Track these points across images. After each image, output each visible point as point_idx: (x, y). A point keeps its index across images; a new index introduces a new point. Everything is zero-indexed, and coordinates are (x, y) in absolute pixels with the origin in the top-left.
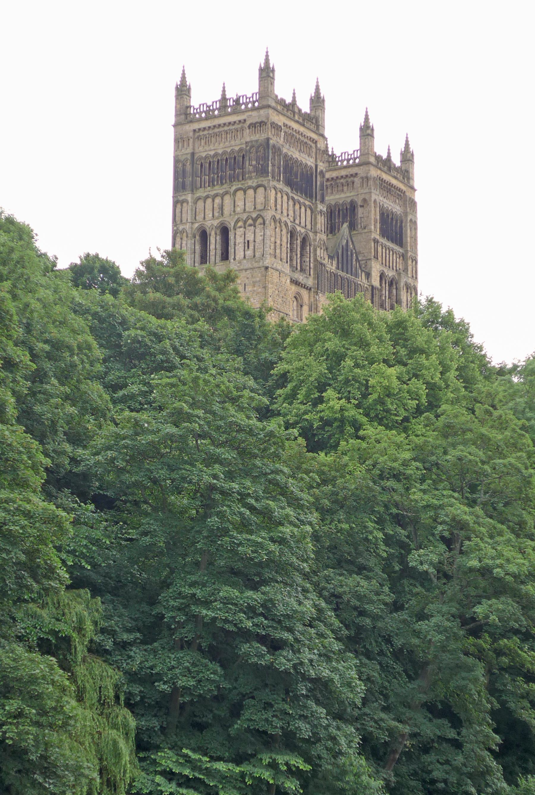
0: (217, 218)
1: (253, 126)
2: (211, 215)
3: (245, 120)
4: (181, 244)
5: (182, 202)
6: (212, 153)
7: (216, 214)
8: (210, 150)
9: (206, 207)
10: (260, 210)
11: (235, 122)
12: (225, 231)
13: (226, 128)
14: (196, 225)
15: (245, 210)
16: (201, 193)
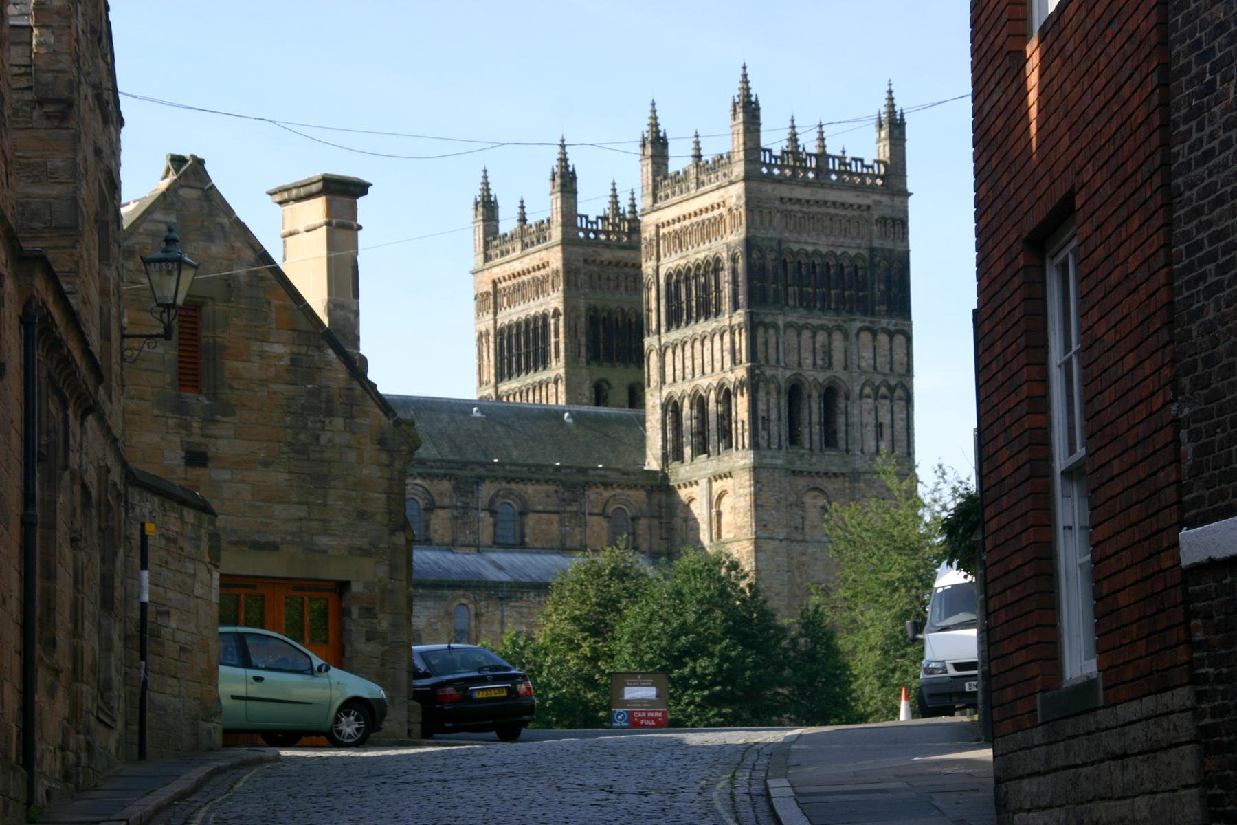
0: (823, 369)
1: (883, 221)
2: (809, 361)
3: (868, 207)
4: (768, 402)
5: (766, 326)
6: (810, 248)
7: (819, 362)
8: (806, 243)
9: (802, 343)
10: (901, 375)
11: (851, 205)
12: (830, 394)
13: (832, 211)
14: (788, 373)
15: (875, 368)
16: (792, 318)
